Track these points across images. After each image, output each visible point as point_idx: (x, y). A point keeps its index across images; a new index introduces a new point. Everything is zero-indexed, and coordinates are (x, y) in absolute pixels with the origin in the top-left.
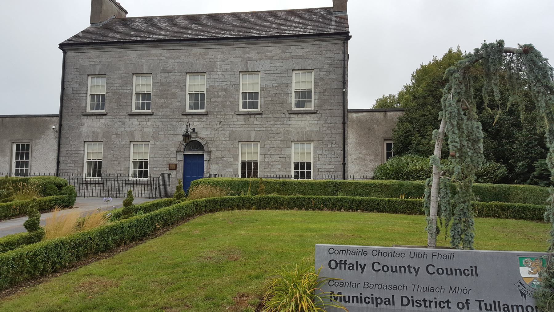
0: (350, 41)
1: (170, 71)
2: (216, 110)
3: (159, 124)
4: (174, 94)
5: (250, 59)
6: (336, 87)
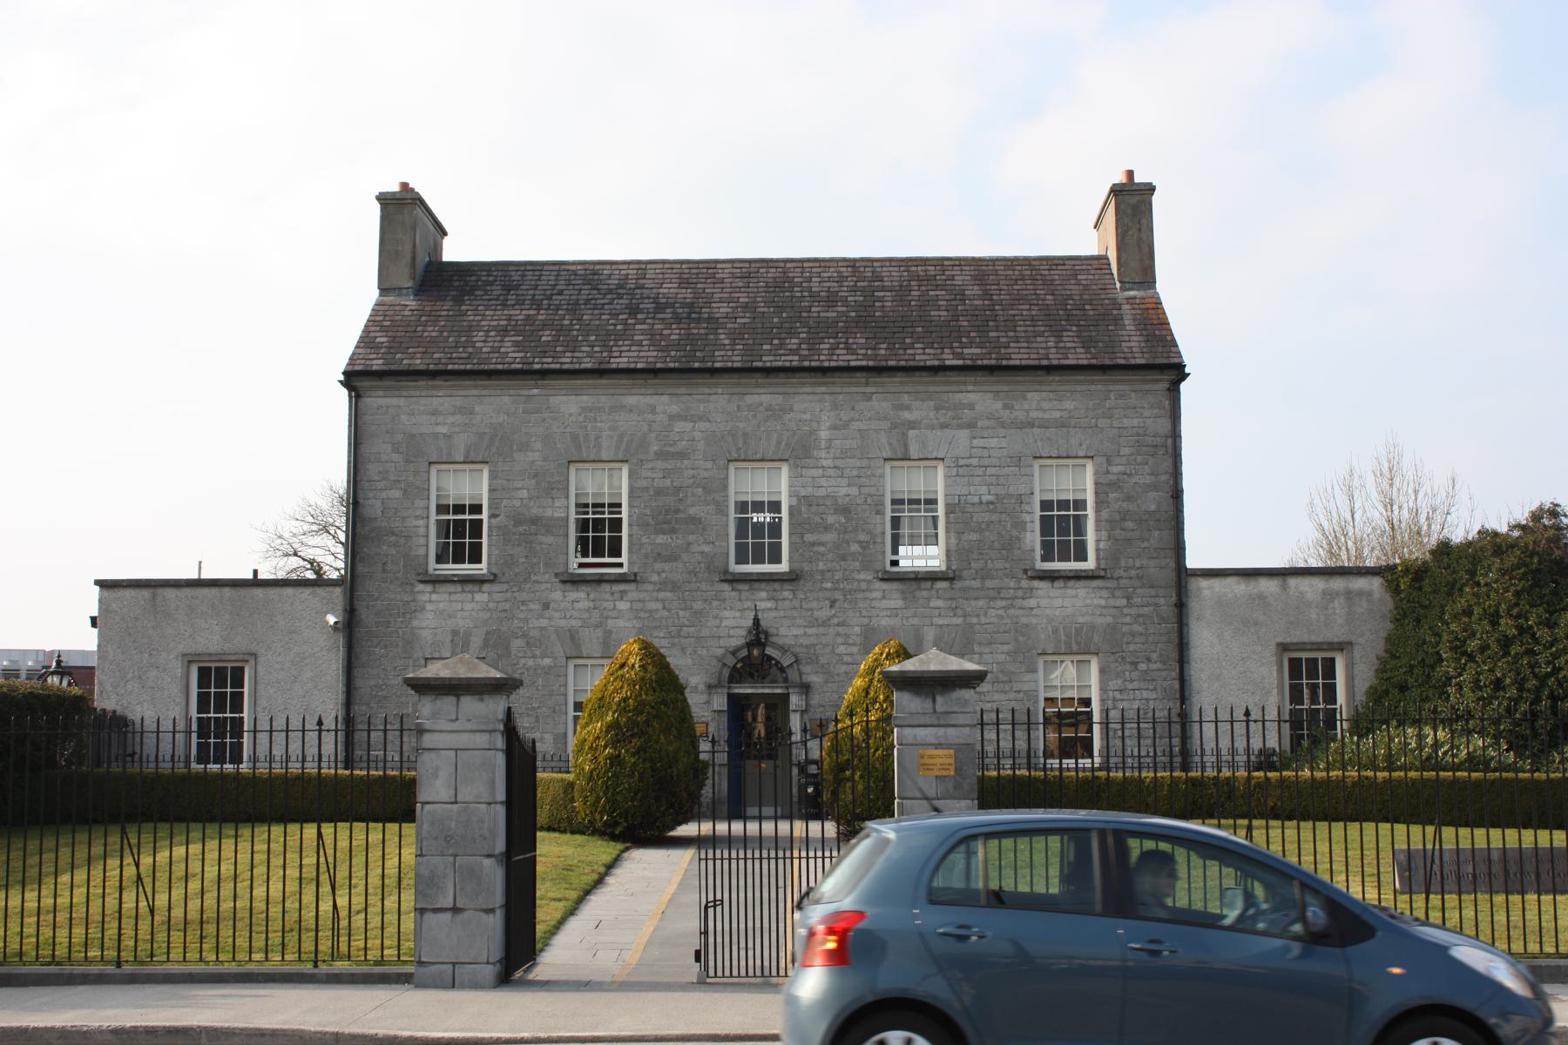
0: (1183, 386)
1: (682, 455)
2: (821, 566)
3: (652, 605)
4: (695, 521)
5: (913, 425)
6: (1153, 508)
